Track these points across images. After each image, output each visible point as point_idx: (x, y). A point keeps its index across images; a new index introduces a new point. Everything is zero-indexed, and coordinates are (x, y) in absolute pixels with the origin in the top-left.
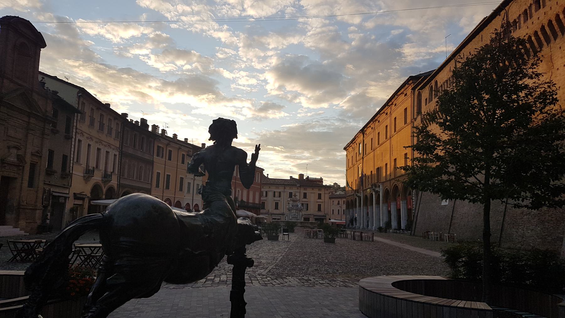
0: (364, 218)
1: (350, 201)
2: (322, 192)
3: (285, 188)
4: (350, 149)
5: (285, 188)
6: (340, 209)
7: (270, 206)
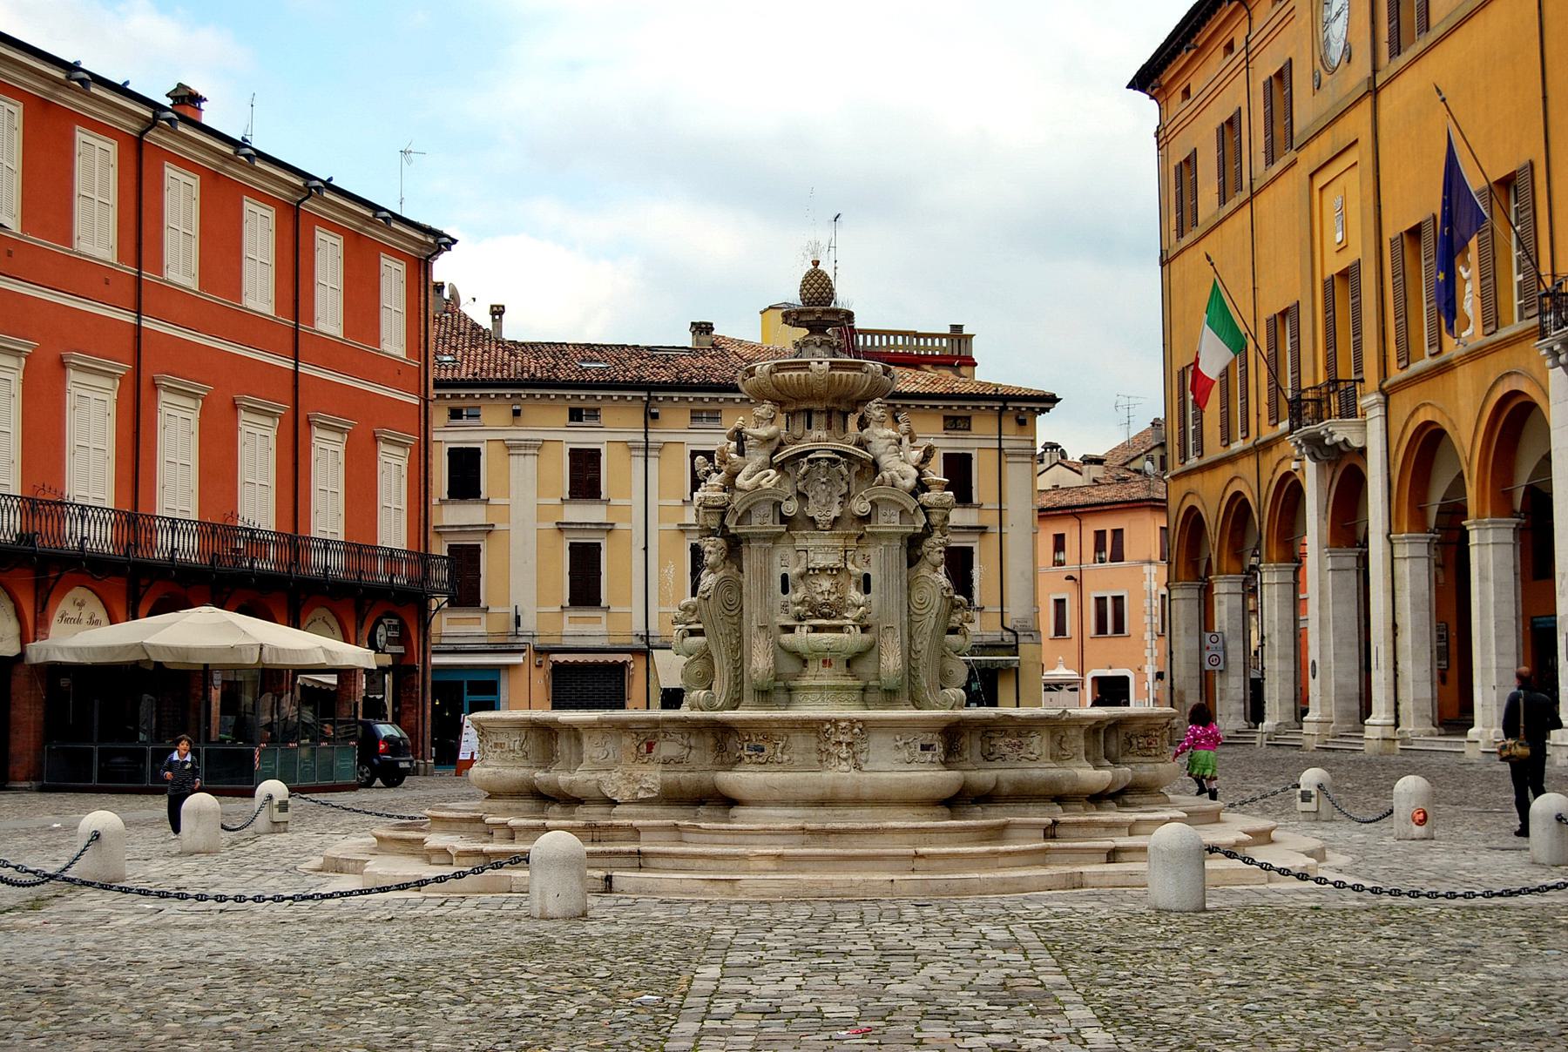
0: (1406, 639)
1: (1212, 515)
2: (978, 443)
3: (651, 417)
4: (1209, 70)
5: (651, 417)
6: (1068, 594)
7: (523, 581)
